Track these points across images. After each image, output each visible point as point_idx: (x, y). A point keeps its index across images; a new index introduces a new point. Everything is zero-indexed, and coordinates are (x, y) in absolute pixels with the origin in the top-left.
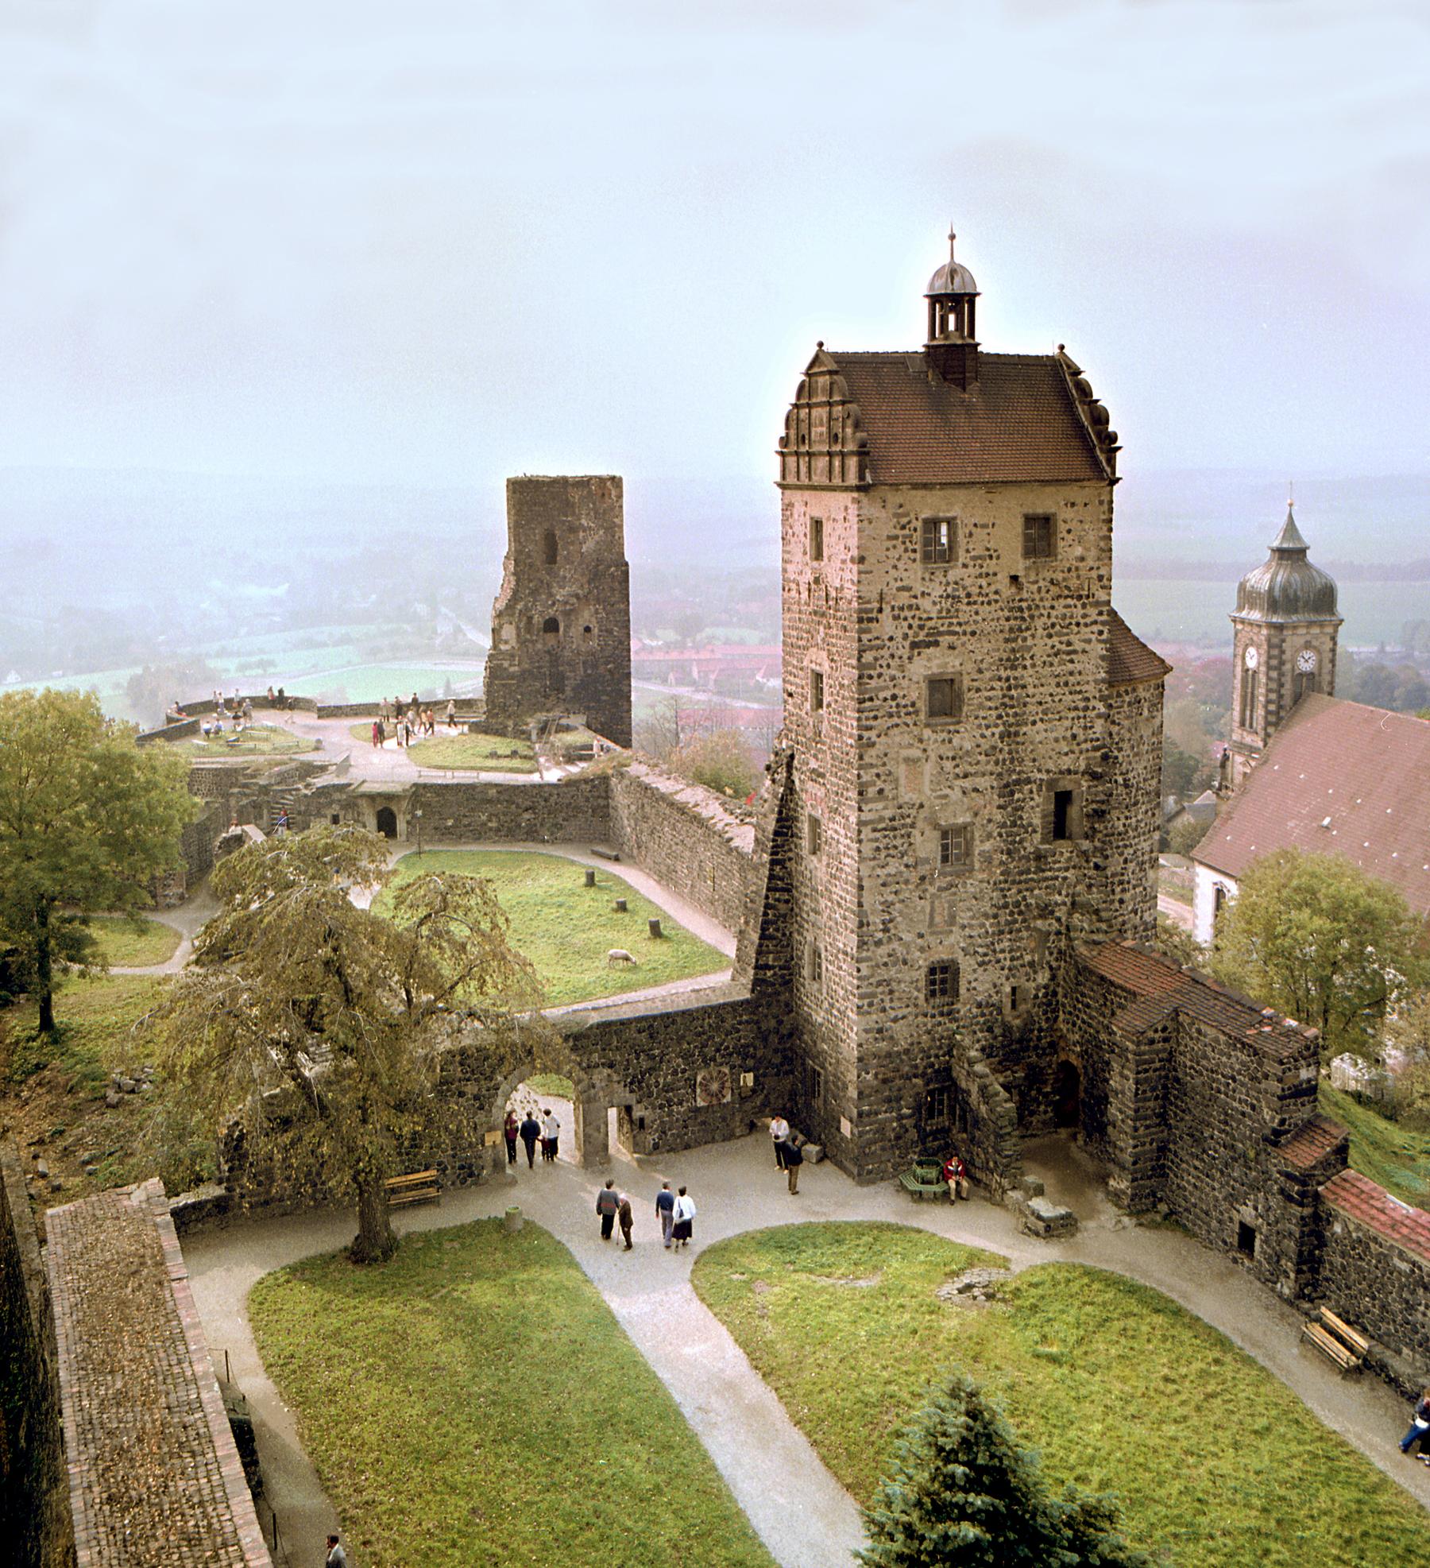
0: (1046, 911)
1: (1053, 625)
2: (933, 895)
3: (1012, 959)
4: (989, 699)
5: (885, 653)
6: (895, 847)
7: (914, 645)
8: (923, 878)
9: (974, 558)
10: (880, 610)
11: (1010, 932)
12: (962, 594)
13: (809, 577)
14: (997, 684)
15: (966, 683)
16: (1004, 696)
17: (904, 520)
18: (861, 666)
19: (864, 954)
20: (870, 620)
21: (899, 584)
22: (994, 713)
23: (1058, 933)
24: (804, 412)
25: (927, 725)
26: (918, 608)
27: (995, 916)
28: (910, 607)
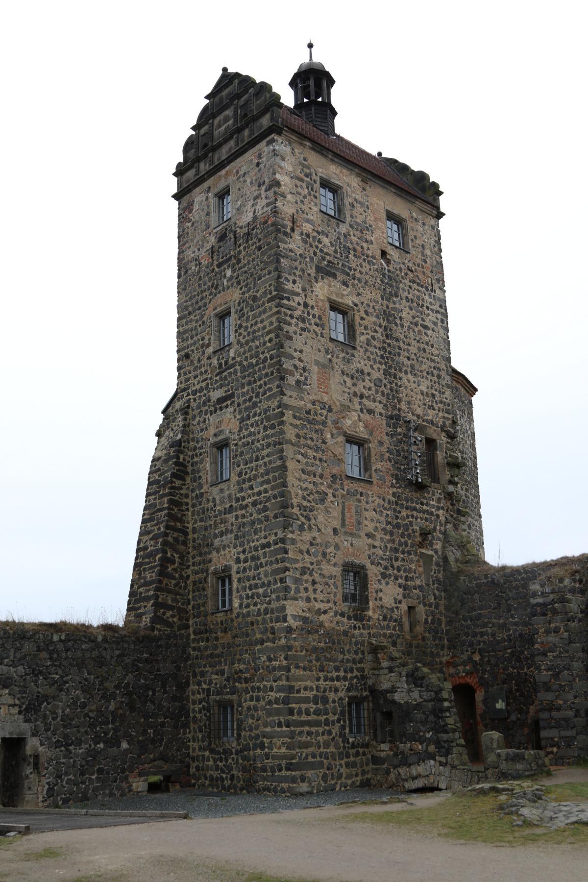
2: (343, 496)
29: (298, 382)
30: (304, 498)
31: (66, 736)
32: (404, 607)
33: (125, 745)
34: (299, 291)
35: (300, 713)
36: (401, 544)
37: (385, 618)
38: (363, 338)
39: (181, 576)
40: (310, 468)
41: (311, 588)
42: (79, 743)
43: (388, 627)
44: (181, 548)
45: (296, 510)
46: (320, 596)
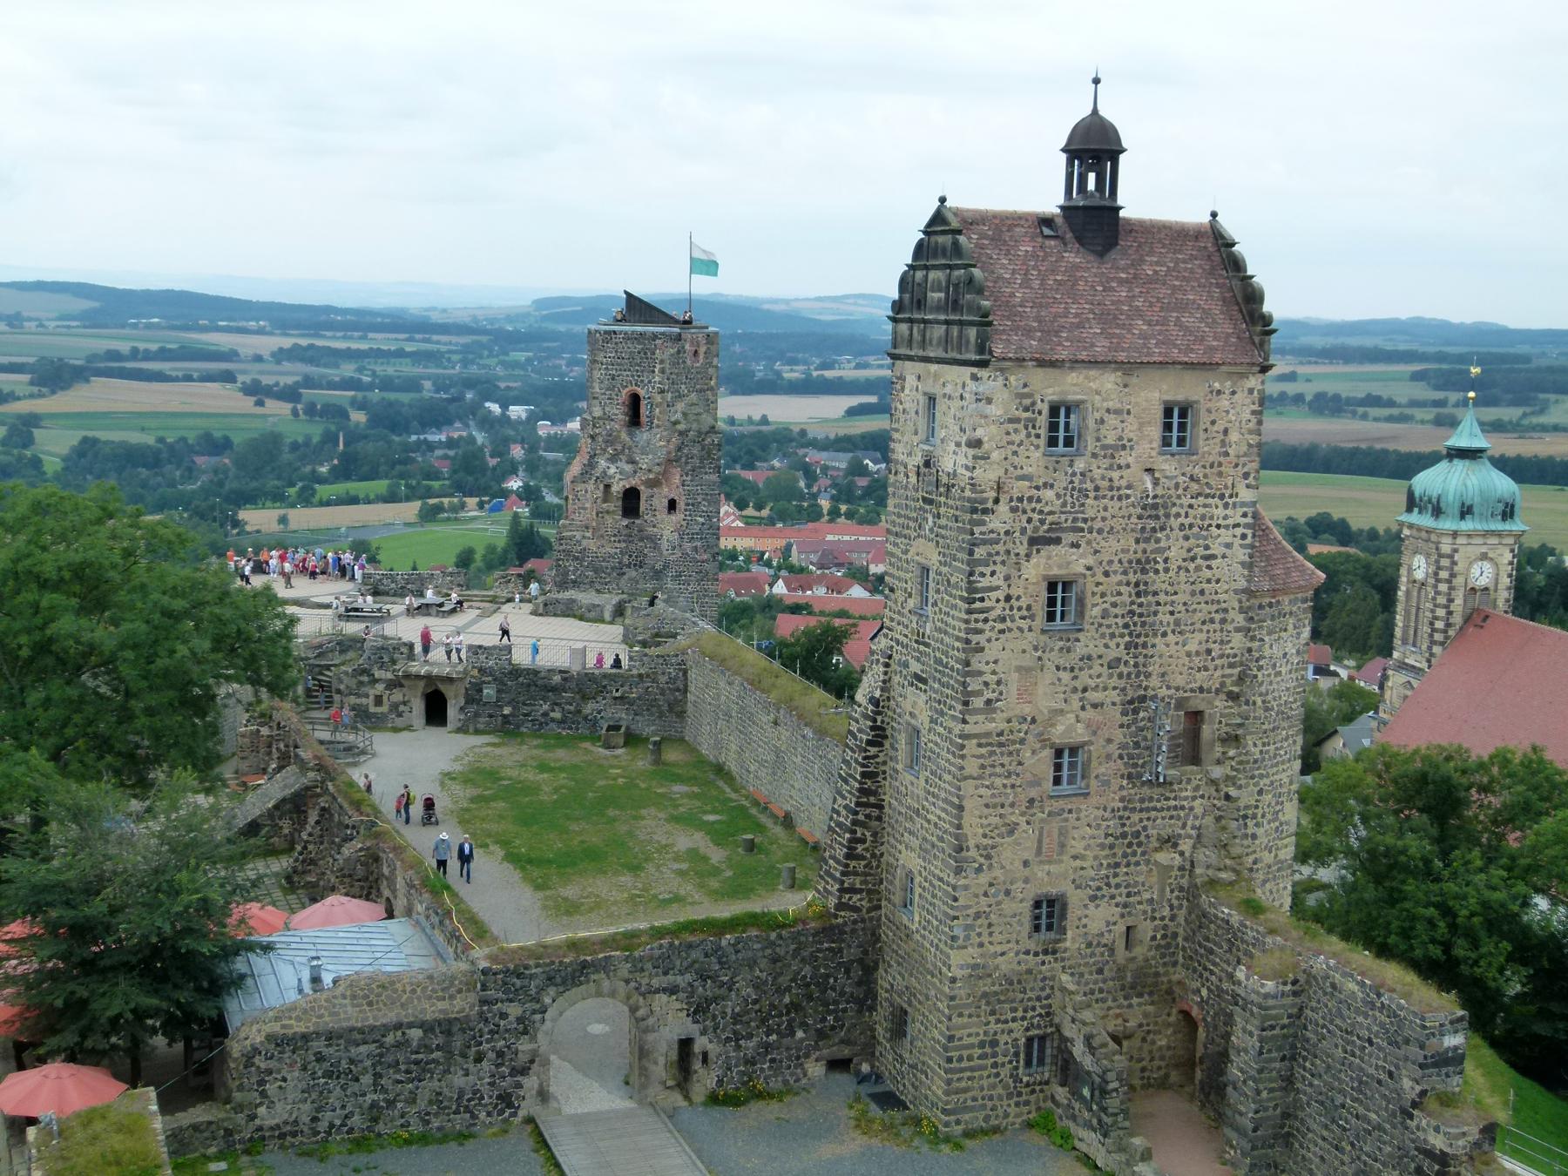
0: (1170, 842)
1: (1191, 526)
2: (1042, 820)
3: (1129, 895)
4: (1114, 605)
5: (1000, 547)
6: (1003, 765)
7: (1033, 541)
8: (1031, 801)
9: (1104, 447)
10: (997, 501)
11: (1128, 865)
12: (1089, 485)
13: (918, 459)
14: (1123, 589)
15: (1090, 587)
16: (1132, 603)
17: (1027, 402)
18: (972, 563)
19: (962, 882)
20: (985, 511)
21: (1019, 472)
22: (1120, 621)
23: (1181, 868)
24: (919, 274)
25: (1043, 632)
26: (1039, 500)
27: (1111, 847)
28: (1030, 499)
29: (989, 702)
30: (985, 836)
31: (735, 1032)
32: (1121, 928)
33: (800, 1034)
34: (1001, 583)
35: (960, 1059)
36: (1125, 855)
37: (1089, 945)
38: (1096, 611)
39: (873, 856)
40: (997, 800)
41: (985, 933)
42: (750, 1036)
43: (1093, 955)
44: (875, 823)
45: (973, 853)
46: (999, 938)
